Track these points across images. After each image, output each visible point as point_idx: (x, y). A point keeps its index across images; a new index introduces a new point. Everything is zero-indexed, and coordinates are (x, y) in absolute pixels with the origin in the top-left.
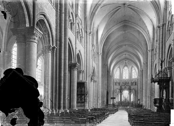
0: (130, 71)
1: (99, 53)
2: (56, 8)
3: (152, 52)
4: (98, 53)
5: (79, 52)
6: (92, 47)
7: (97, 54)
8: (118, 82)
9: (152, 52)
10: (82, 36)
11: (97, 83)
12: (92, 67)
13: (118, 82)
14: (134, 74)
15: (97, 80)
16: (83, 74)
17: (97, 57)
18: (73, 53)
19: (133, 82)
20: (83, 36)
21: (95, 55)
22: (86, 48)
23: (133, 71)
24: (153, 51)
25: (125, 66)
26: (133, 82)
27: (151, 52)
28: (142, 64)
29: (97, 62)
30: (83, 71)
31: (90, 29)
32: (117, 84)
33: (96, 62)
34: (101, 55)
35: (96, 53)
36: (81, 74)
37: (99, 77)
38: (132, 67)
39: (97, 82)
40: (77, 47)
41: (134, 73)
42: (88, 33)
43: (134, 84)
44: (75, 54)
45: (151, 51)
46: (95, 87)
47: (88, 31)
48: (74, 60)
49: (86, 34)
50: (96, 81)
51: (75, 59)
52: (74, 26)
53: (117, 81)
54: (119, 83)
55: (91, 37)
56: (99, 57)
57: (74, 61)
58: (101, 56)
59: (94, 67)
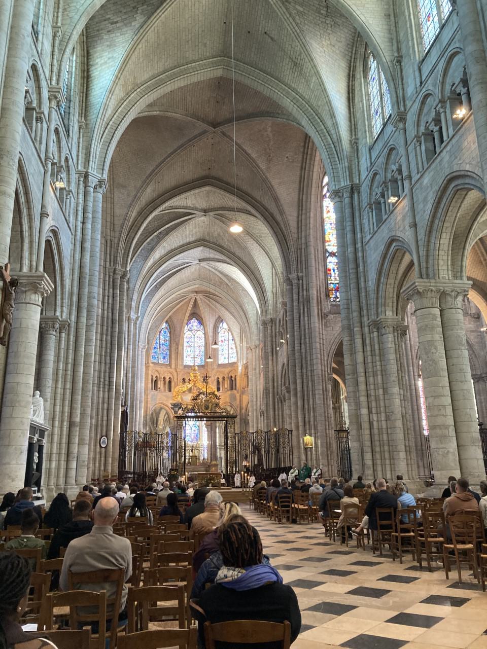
0: (210, 334)
1: (93, 181)
3: (352, 198)
4: (86, 176)
8: (164, 378)
9: (352, 198)
11: (72, 338)
13: (164, 378)
14: (225, 348)
15: (73, 318)
17: (81, 197)
19: (221, 380)
23: (223, 334)
24: (356, 194)
25: (190, 319)
26: (224, 378)
27: (347, 200)
28: (269, 295)
29: (80, 225)
32: (160, 384)
34: (101, 190)
37: (85, 304)
38: (220, 320)
39: (73, 330)
41: (226, 343)
43: (227, 384)
45: (346, 195)
50: (64, 326)
53: (162, 372)
54: (170, 382)
56: (91, 199)
58: (100, 196)
59: (55, 232)
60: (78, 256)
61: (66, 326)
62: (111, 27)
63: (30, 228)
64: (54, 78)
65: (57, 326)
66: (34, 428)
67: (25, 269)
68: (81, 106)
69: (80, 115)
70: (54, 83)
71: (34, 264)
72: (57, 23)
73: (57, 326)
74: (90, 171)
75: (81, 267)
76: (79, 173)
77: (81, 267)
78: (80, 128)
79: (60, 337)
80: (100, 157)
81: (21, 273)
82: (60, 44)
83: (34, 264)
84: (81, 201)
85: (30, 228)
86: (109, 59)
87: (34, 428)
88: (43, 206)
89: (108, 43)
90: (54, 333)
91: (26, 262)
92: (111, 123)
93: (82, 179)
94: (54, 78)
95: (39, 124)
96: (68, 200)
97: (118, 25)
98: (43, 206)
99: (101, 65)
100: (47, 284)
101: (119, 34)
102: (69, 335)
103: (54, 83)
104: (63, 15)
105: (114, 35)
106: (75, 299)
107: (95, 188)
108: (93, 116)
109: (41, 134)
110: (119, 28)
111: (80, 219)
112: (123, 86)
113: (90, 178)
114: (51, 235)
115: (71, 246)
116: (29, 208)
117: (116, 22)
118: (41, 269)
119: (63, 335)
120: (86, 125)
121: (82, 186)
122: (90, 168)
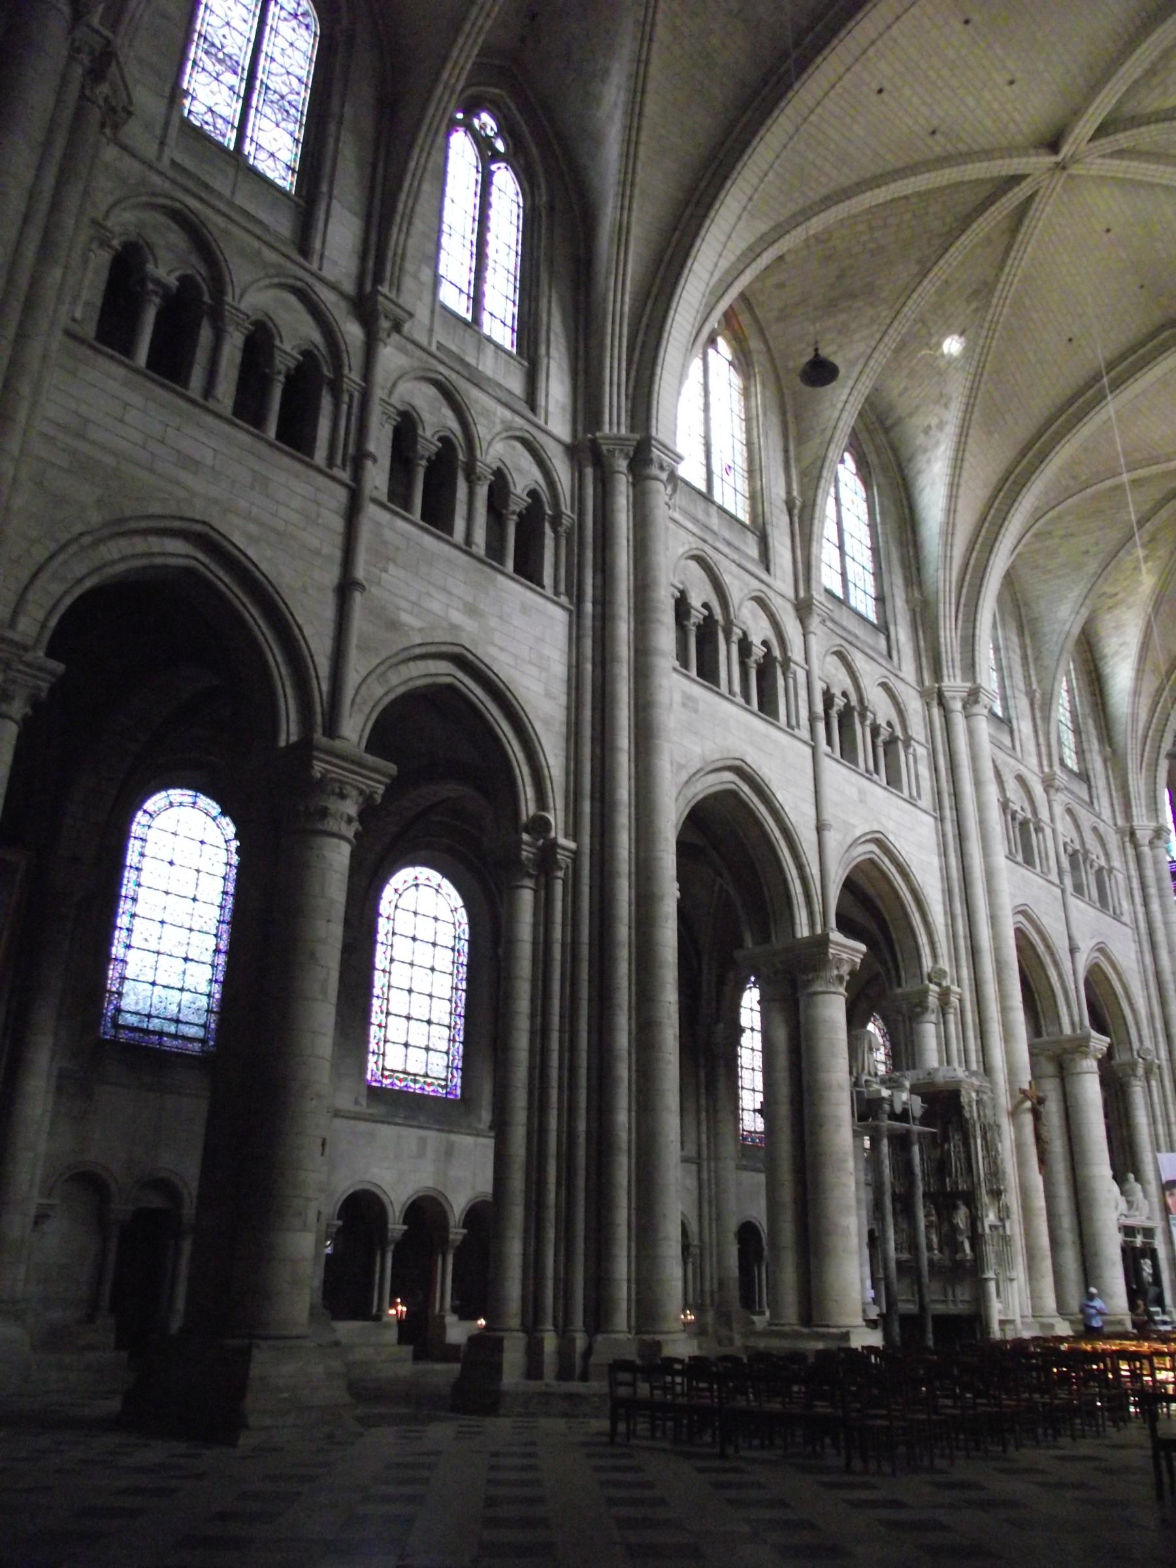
2: (571, 602)
4: (1132, 834)
5: (873, 847)
6: (1046, 791)
7: (1128, 845)
10: (905, 728)
12: (1073, 950)
16: (951, 1018)
17: (1132, 866)
18: (800, 867)
20: (917, 730)
21: (1107, 855)
22: (948, 813)
29: (1140, 910)
30: (944, 995)
31: (970, 667)
33: (1125, 905)
35: (1113, 840)
36: (933, 1017)
40: (828, 815)
42: (958, 705)
44: (814, 870)
46: (1155, 1122)
47: (954, 684)
48: (811, 914)
49: (936, 711)
51: (818, 908)
52: (791, 681)
55: (984, 727)
57: (812, 925)
60: (1148, 959)
61: (1156, 1070)
62: (1110, 602)
63: (1060, 976)
64: (1045, 763)
65: (1140, 1071)
66: (1128, 1231)
67: (1067, 1030)
68: (1098, 728)
69: (1101, 741)
70: (1046, 769)
71: (1076, 1018)
72: (1030, 685)
73: (1140, 1071)
74: (1135, 823)
75: (1158, 974)
76: (1119, 831)
77: (1158, 974)
78: (1105, 761)
79: (1149, 1086)
80: (1147, 792)
81: (1062, 1038)
82: (1042, 710)
83: (1076, 1018)
84: (1134, 872)
85: (1060, 976)
86: (1121, 645)
87: (1128, 1231)
88: (1070, 938)
89: (1112, 624)
90: (1139, 1083)
91: (1065, 1020)
92: (1151, 733)
93: (1127, 839)
94: (1045, 763)
95: (1041, 836)
96: (1113, 881)
97: (1120, 596)
98: (1070, 938)
99: (1112, 656)
100: (1099, 1042)
101: (1124, 609)
102: (1162, 1081)
103: (1046, 769)
104: (1036, 669)
105: (1116, 612)
106: (1159, 1025)
107: (1151, 843)
108: (1119, 738)
109: (1046, 848)
110: (1122, 601)
111: (1138, 899)
112: (1153, 671)
113: (1139, 834)
114: (1097, 954)
115: (1133, 947)
116: (1052, 954)
117: (1116, 595)
118: (1087, 1022)
119: (1153, 1083)
120: (1114, 752)
121: (1130, 850)
122: (1135, 818)
